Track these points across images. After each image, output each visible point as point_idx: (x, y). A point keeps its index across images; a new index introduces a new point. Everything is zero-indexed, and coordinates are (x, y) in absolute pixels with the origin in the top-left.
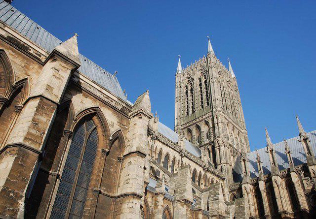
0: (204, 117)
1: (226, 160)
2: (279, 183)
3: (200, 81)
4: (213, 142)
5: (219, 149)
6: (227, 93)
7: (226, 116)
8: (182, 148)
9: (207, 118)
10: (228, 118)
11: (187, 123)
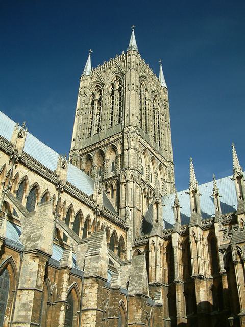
0: (111, 139)
1: (134, 202)
2: (197, 236)
3: (113, 88)
4: (119, 176)
6: (151, 108)
7: (143, 140)
9: (114, 141)
10: (146, 144)
11: (87, 147)
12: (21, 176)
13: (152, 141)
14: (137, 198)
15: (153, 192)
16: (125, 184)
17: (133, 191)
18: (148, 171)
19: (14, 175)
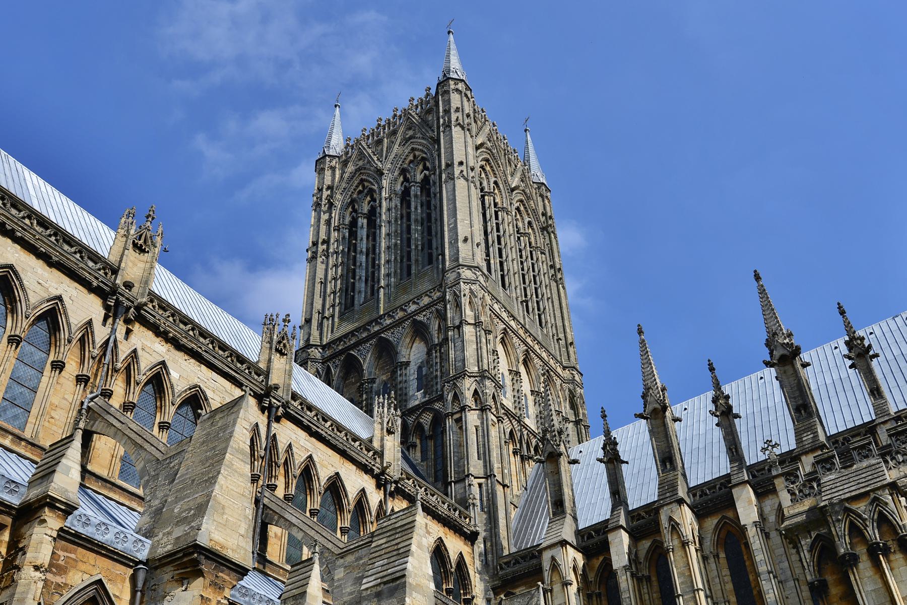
0: (413, 308)
4: (441, 398)
5: (459, 421)
7: (496, 307)
8: (274, 379)
9: (417, 312)
10: (504, 315)
12: (146, 362)
13: (518, 311)
14: (495, 453)
15: (534, 441)
16: (456, 416)
17: (480, 433)
18: (516, 387)
19: (122, 356)
